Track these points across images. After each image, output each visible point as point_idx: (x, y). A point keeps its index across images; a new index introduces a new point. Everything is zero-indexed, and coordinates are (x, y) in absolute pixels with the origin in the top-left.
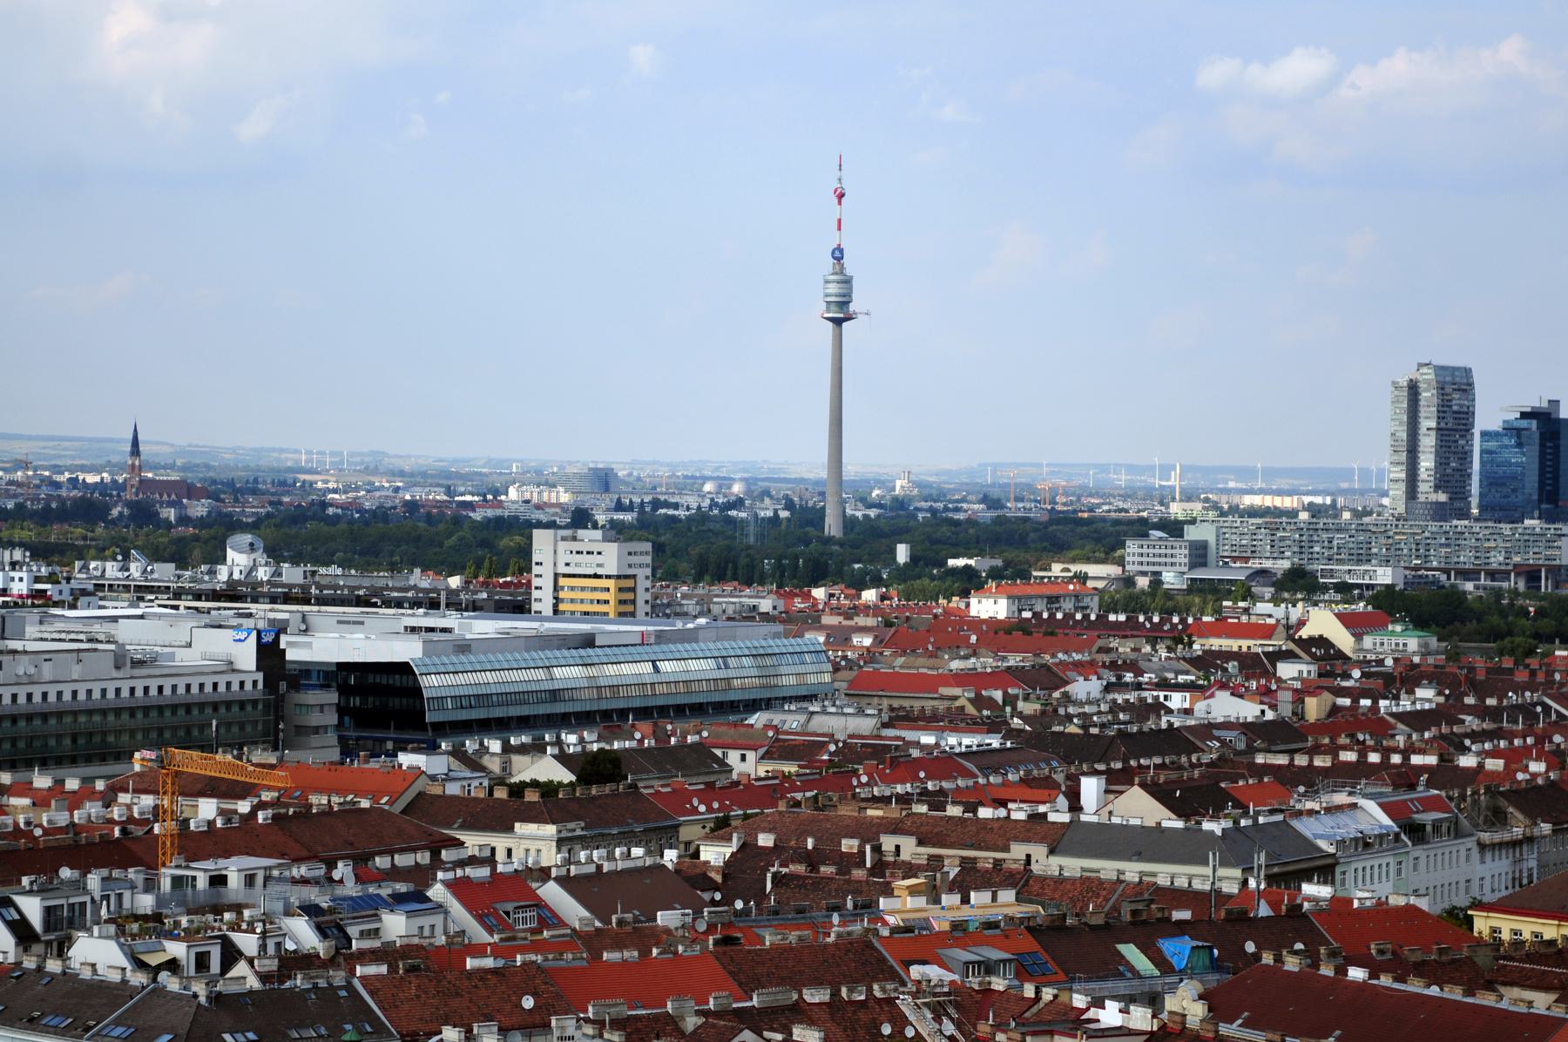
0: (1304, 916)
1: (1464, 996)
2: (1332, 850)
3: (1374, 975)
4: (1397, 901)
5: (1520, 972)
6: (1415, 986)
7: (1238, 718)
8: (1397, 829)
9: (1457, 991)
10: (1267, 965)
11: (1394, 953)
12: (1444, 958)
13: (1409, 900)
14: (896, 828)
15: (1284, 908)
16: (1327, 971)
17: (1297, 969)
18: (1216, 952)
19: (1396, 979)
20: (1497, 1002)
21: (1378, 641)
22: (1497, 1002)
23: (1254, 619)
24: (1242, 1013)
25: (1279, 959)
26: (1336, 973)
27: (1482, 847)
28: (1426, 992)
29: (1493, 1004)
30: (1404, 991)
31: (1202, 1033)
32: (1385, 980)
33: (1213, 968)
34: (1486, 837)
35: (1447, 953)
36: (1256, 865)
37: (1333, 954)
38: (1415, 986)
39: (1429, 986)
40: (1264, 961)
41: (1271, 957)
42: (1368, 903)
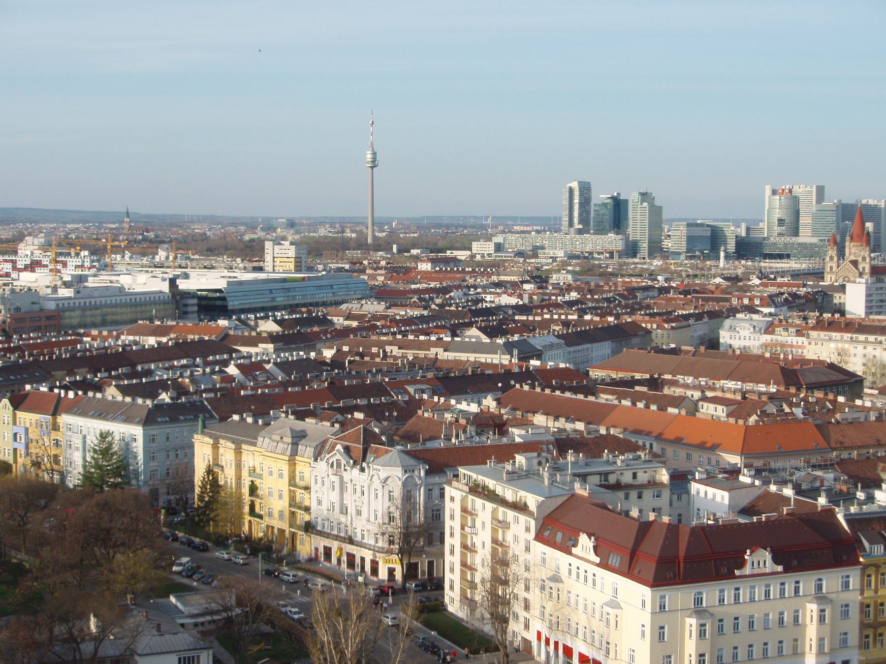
2: (541, 348)
4: (562, 365)
14: (391, 343)
19: (561, 393)
25: (521, 386)
38: (568, 394)
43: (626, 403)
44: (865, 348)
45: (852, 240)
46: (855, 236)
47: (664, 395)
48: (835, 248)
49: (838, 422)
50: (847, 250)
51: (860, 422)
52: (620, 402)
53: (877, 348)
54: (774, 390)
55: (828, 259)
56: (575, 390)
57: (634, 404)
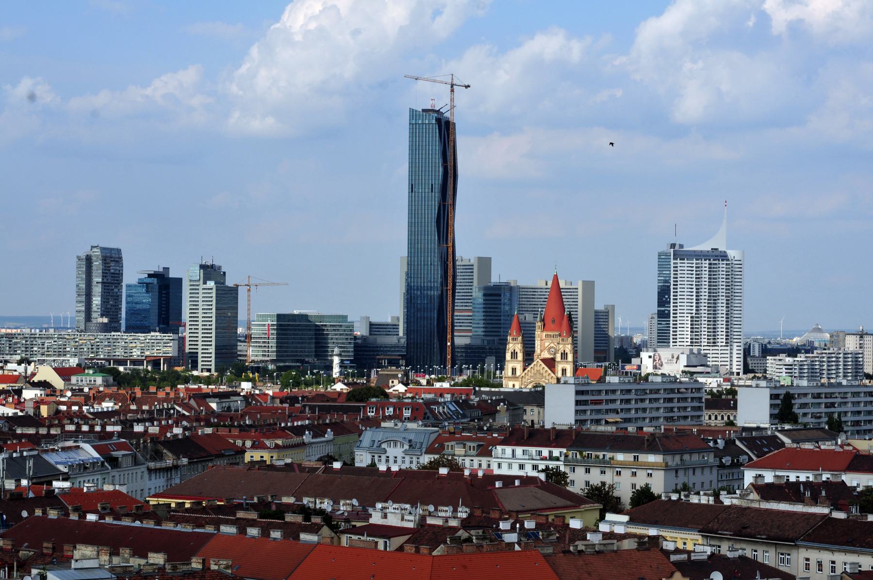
0: (56, 497)
1: (155, 525)
2: (66, 470)
3: (102, 517)
4: (108, 488)
5: (183, 518)
6: (126, 522)
7: (3, 414)
8: (102, 460)
9: (151, 523)
10: (38, 517)
11: (111, 509)
12: (140, 512)
13: (115, 487)
15: (44, 492)
16: (74, 517)
17: (56, 517)
18: (5, 516)
19: (115, 519)
20: (174, 527)
21: (79, 379)
22: (174, 527)
23: (6, 373)
24: (24, 544)
25: (45, 512)
26: (79, 518)
27: (150, 470)
28: (133, 524)
29: (172, 528)
30: (120, 525)
31: (4, 547)
32: (109, 520)
33: (3, 526)
34: (152, 465)
35: (141, 509)
36: (27, 467)
37: (76, 510)
38: (126, 522)
39: (134, 521)
40: (36, 514)
41: (41, 511)
42: (92, 489)
43: (228, 530)
44: (588, 471)
46: (548, 321)
47: (286, 523)
48: (520, 338)
49: (580, 552)
50: (538, 343)
51: (614, 551)
52: (218, 529)
53: (607, 470)
54: (464, 516)
55: (508, 356)
56: (136, 517)
57: (242, 531)
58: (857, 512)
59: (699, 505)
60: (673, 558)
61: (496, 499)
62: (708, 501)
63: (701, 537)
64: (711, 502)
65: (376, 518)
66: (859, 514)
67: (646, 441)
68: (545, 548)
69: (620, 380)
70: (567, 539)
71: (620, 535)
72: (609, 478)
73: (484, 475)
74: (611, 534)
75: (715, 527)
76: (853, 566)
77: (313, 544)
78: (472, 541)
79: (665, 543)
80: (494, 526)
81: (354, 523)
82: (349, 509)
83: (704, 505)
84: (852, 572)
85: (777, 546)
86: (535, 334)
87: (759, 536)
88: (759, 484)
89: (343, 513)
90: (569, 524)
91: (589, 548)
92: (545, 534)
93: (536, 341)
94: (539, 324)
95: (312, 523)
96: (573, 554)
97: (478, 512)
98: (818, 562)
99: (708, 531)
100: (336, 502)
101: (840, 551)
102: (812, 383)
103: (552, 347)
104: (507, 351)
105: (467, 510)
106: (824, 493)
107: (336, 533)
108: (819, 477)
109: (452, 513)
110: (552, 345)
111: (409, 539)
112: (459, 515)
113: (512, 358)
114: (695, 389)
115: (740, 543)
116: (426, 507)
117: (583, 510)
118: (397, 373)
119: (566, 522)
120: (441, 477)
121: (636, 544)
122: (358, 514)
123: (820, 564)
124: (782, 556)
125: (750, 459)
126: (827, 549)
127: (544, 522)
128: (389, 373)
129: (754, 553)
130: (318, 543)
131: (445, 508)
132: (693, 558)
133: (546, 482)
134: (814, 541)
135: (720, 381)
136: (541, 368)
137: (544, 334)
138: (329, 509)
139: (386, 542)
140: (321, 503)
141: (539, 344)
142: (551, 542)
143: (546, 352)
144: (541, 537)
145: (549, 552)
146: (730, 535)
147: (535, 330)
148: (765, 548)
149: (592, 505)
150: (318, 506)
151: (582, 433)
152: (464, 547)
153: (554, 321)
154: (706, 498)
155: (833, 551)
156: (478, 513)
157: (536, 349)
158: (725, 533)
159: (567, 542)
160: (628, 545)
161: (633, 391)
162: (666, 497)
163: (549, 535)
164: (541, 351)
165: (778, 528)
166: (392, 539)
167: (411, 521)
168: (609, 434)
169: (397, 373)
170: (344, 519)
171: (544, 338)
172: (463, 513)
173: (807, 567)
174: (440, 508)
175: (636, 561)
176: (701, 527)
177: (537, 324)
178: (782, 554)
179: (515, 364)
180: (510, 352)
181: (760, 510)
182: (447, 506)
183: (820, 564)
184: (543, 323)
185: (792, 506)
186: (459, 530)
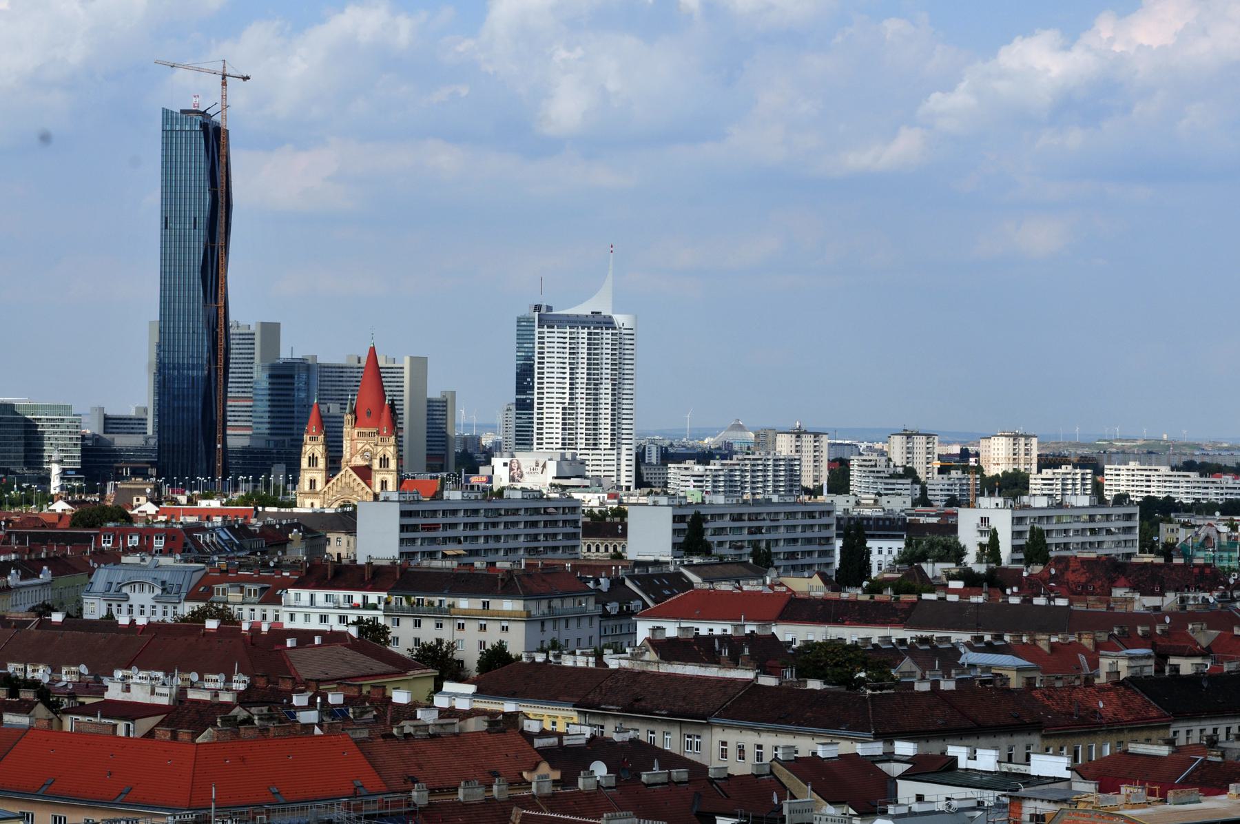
44: (417, 624)
45: (356, 422)
46: (362, 413)
48: (321, 437)
49: (408, 736)
50: (346, 444)
53: (445, 622)
54: (242, 687)
55: (304, 463)
58: (792, 676)
59: (575, 670)
60: (538, 743)
61: (288, 664)
62: (587, 663)
63: (576, 713)
64: (591, 665)
65: (114, 692)
66: (796, 680)
67: (499, 581)
68: (358, 731)
69: (463, 496)
70: (389, 719)
71: (464, 712)
72: (447, 633)
73: (270, 630)
74: (451, 711)
75: (597, 700)
76: (787, 751)
77: (22, 729)
78: (253, 723)
79: (526, 722)
80: (285, 701)
81: (81, 700)
82: (74, 680)
83: (581, 669)
84: (785, 759)
85: (682, 725)
86: (342, 432)
87: (657, 712)
88: (658, 638)
89: (66, 685)
90: (391, 698)
91: (420, 731)
92: (358, 711)
93: (344, 442)
94: (349, 417)
95: (21, 700)
96: (398, 739)
97: (262, 682)
98: (739, 746)
99: (587, 705)
100: (56, 669)
101: (769, 731)
102: (730, 499)
103: (367, 451)
104: (303, 456)
105: (246, 678)
106: (747, 651)
107: (55, 713)
108: (740, 629)
109: (224, 684)
110: (367, 447)
111: (162, 721)
112: (235, 686)
113: (310, 465)
114: (569, 508)
115: (631, 721)
116: (186, 676)
117: (411, 678)
118: (144, 487)
119: (388, 694)
120: (209, 634)
121: (486, 724)
122: (87, 686)
123: (741, 750)
124: (689, 739)
125: (645, 605)
126: (752, 729)
127: (356, 694)
128: (132, 487)
129: (650, 735)
130: (30, 728)
131: (216, 677)
132: (565, 743)
133: (359, 638)
134: (733, 718)
135: (604, 497)
136: (352, 479)
137: (356, 431)
138: (46, 680)
139: (129, 725)
140: (34, 671)
141: (349, 445)
142: (365, 723)
143: (359, 456)
144: (351, 716)
145: (362, 736)
146: (618, 711)
147: (342, 427)
148: (666, 729)
149: (424, 671)
150: (29, 676)
151: (410, 570)
152: (242, 731)
153: (369, 413)
154: (584, 659)
155: (759, 731)
156: (261, 683)
157: (344, 453)
158: (611, 707)
159: (388, 723)
160: (474, 725)
161: (482, 511)
162: (528, 658)
163: (362, 713)
164: (352, 455)
165: (684, 699)
166: (136, 721)
167: (165, 695)
168: (447, 571)
169: (144, 487)
170: (68, 694)
171: (356, 437)
172: (240, 683)
173: (724, 754)
174: (207, 676)
175: (485, 748)
176: (577, 700)
177: (345, 418)
178: (689, 736)
179: (315, 475)
180: (307, 457)
181: (660, 676)
182: (217, 673)
183: (741, 750)
184: (354, 416)
185: (703, 669)
186: (235, 707)
